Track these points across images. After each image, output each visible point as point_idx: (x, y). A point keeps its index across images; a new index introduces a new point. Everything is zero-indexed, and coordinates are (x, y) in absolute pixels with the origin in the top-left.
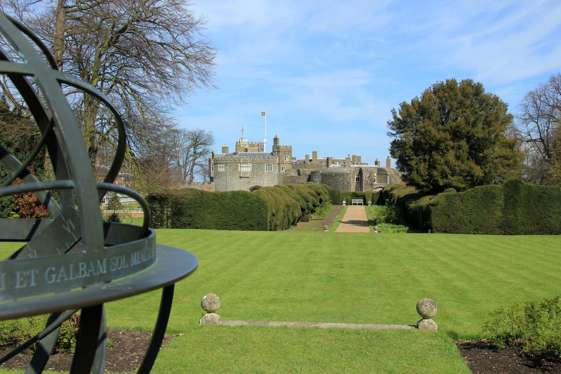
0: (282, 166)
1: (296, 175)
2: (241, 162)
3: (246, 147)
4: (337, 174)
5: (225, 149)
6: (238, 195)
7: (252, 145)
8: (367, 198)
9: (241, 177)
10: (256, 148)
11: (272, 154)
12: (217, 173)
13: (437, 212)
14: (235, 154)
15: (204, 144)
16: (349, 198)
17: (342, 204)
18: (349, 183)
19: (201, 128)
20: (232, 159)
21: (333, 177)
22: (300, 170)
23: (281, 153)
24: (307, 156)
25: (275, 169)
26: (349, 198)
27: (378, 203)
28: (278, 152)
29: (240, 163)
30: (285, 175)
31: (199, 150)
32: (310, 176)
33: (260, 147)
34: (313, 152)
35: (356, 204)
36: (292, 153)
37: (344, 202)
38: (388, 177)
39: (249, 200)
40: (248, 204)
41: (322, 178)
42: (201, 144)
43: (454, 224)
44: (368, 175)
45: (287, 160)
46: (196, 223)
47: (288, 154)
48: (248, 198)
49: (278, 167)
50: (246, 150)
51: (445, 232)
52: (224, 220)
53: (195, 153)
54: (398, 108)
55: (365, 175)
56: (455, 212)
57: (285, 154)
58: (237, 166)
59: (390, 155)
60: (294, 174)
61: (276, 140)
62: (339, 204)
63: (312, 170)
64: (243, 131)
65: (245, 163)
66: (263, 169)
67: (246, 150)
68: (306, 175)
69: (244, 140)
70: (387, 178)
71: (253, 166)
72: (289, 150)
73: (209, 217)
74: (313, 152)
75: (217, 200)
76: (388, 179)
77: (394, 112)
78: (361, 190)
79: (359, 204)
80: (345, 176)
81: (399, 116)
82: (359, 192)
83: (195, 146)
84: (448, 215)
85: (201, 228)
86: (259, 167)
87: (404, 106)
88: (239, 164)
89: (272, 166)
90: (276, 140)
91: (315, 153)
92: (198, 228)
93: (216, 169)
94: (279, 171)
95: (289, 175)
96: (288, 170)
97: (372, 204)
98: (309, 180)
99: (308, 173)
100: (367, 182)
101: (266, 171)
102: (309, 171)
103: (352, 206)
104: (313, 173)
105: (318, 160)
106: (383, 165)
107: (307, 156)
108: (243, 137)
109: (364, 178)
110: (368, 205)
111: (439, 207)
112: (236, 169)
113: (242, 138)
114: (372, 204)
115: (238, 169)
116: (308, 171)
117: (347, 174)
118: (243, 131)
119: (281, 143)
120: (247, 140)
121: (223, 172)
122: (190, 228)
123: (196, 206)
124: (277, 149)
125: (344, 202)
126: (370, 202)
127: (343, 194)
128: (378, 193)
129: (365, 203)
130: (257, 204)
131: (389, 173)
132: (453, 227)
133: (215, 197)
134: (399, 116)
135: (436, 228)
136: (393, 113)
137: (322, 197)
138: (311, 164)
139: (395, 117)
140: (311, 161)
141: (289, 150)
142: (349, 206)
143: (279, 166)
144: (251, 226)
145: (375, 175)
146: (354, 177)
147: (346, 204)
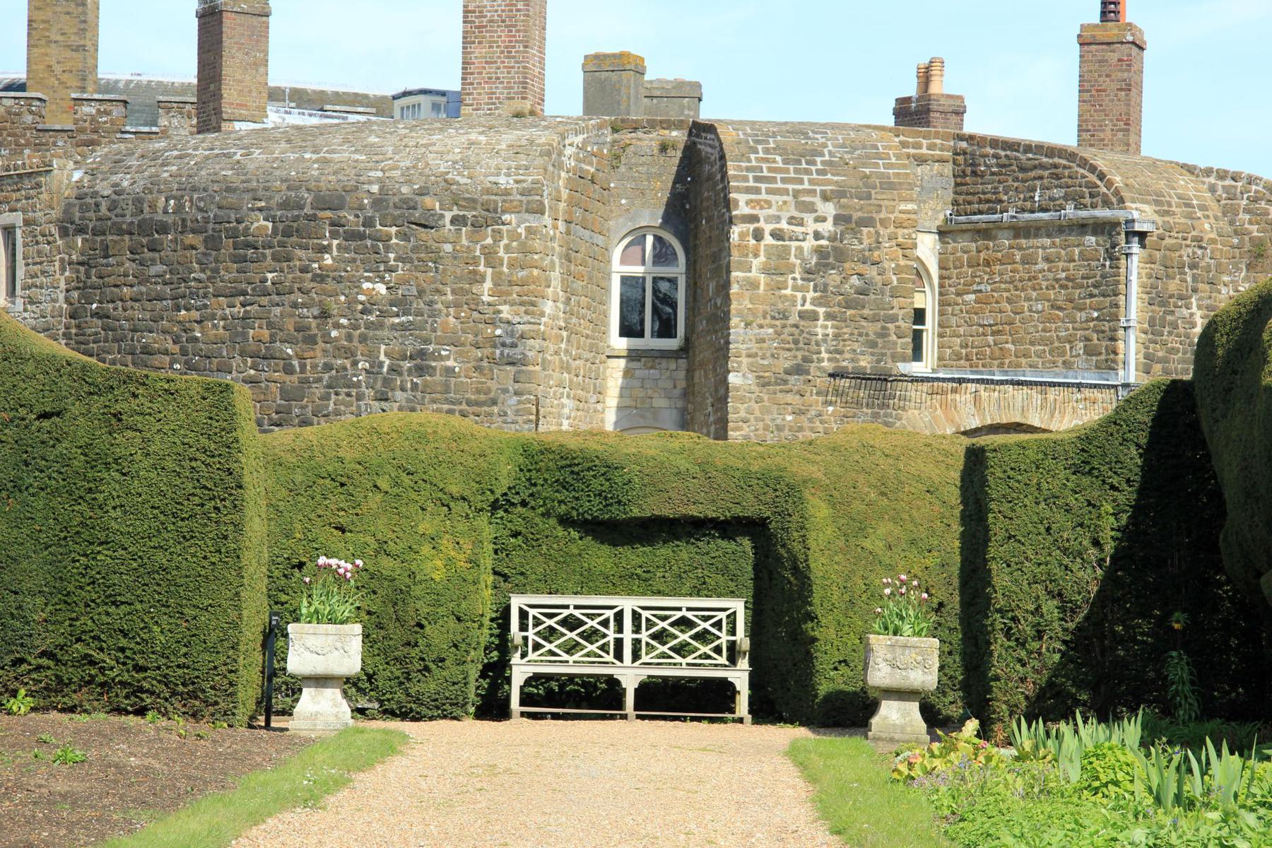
4: (309, 215)
8: (825, 563)
16: (449, 555)
17: (278, 692)
18: (508, 354)
21: (248, 250)
26: (449, 555)
27: (1098, 677)
35: (597, 698)
37: (326, 647)
38: (1136, 266)
44: (822, 223)
55: (771, 230)
62: (196, 696)
70: (1108, 288)
76: (1135, 308)
78: (703, 404)
79: (664, 699)
80: (451, 239)
82: (667, 463)
97: (972, 694)
100: (801, 340)
103: (520, 734)
106: (1026, 100)
109: (748, 274)
110: (851, 712)
114: (972, 694)
117: (482, 213)
125: (326, 647)
126: (907, 659)
127: (333, 490)
128: (1086, 453)
129: (795, 685)
131: (1142, 215)
142: (451, 746)
145: (927, 248)
146: (583, 264)
147: (394, 690)
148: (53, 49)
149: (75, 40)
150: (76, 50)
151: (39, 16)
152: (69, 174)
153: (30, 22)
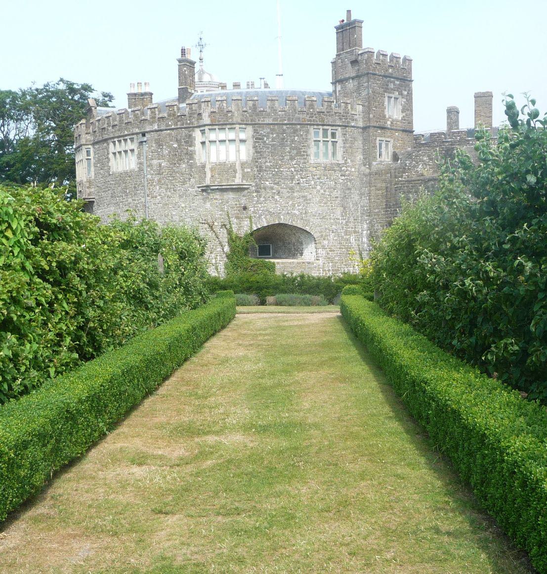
2: (206, 120)
5: (139, 98)
9: (206, 189)
24: (453, 114)
25: (348, 152)
34: (478, 96)
36: (414, 86)
47: (398, 89)
49: (359, 143)
57: (387, 90)
58: (190, 141)
61: (348, 31)
66: (300, 152)
71: (258, 138)
74: (478, 96)
86: (283, 145)
89: (339, 138)
90: (348, 31)
91: (483, 101)
96: (409, 156)
101: (312, 159)
105: (494, 128)
107: (453, 114)
112: (183, 153)
115: (191, 155)
119: (372, 40)
121: (128, 174)
143: (365, 141)
148: (482, 118)
149: (488, 115)
150: (489, 117)
151: (478, 109)
153: (475, 111)
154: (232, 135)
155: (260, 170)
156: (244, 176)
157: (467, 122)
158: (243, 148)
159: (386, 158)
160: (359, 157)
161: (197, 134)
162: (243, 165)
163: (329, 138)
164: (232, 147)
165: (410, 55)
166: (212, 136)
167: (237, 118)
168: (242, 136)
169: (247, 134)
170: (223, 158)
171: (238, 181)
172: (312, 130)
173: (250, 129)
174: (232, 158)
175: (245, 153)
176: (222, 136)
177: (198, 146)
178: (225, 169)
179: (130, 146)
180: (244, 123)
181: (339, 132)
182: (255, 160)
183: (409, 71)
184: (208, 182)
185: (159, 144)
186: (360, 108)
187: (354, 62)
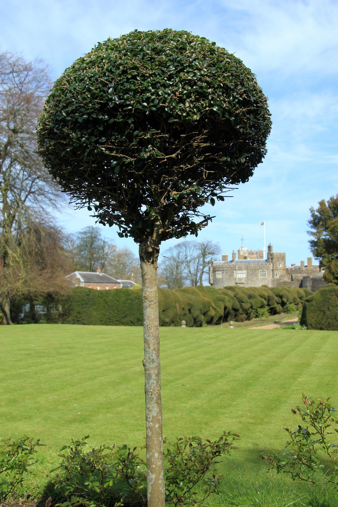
0: (276, 272)
1: (290, 281)
2: (237, 268)
3: (245, 255)
6: (121, 292)
7: (251, 253)
10: (255, 256)
11: (266, 261)
12: (215, 279)
13: (312, 308)
14: (231, 262)
15: (212, 253)
19: (209, 239)
20: (230, 268)
22: (293, 275)
23: (275, 260)
24: (302, 262)
25: (269, 275)
28: (272, 259)
29: (236, 270)
30: (278, 280)
31: (207, 260)
32: (302, 281)
33: (260, 255)
39: (130, 297)
40: (129, 301)
41: (313, 283)
42: (209, 253)
43: (330, 320)
45: (281, 266)
46: (83, 319)
47: (282, 260)
48: (129, 295)
49: (271, 273)
50: (245, 258)
51: (321, 329)
52: (107, 317)
53: (204, 262)
54: (317, 207)
56: (330, 308)
57: (278, 260)
58: (233, 273)
59: (311, 255)
60: (287, 279)
61: (269, 247)
63: (305, 275)
64: (242, 240)
65: (240, 269)
66: (257, 275)
67: (245, 258)
68: (298, 280)
69: (243, 249)
71: (248, 273)
72: (282, 257)
73: (95, 313)
75: (102, 298)
77: (312, 211)
81: (317, 213)
83: (204, 255)
84: (323, 311)
85: (88, 324)
86: (253, 273)
87: (322, 203)
88: (235, 271)
89: (266, 273)
92: (85, 324)
93: (214, 276)
94: (273, 277)
95: (283, 281)
98: (301, 286)
99: (301, 278)
101: (260, 277)
102: (301, 276)
104: (305, 278)
105: (313, 266)
107: (302, 262)
108: (243, 245)
111: (314, 303)
112: (232, 275)
113: (242, 247)
115: (233, 276)
116: (300, 276)
118: (242, 240)
119: (275, 251)
120: (246, 249)
121: (220, 279)
122: (79, 324)
123: (83, 303)
124: (271, 256)
130: (137, 301)
132: (329, 324)
133: (100, 295)
134: (317, 213)
135: (311, 325)
136: (311, 212)
137: (285, 300)
138: (306, 270)
139: (313, 215)
140: (306, 266)
141: (282, 257)
144: (132, 322)
152: (311, 277)
154: (242, 272)
155: (248, 279)
156: (244, 281)
157: (306, 264)
158: (244, 275)
159: (278, 277)
160: (271, 276)
161: (235, 271)
162: (244, 278)
163: (264, 272)
164: (242, 275)
165: (285, 252)
166: (238, 272)
167: (243, 268)
168: (244, 272)
169: (245, 271)
170: (240, 277)
171: (243, 281)
172: (260, 271)
173: (246, 271)
174: (242, 277)
175: (244, 276)
176: (240, 272)
177: (235, 274)
178: (241, 279)
179: (221, 272)
180: (245, 269)
181: (266, 271)
182: (247, 277)
183: (285, 256)
184: (237, 281)
185: (227, 273)
186: (272, 265)
187: (271, 255)
